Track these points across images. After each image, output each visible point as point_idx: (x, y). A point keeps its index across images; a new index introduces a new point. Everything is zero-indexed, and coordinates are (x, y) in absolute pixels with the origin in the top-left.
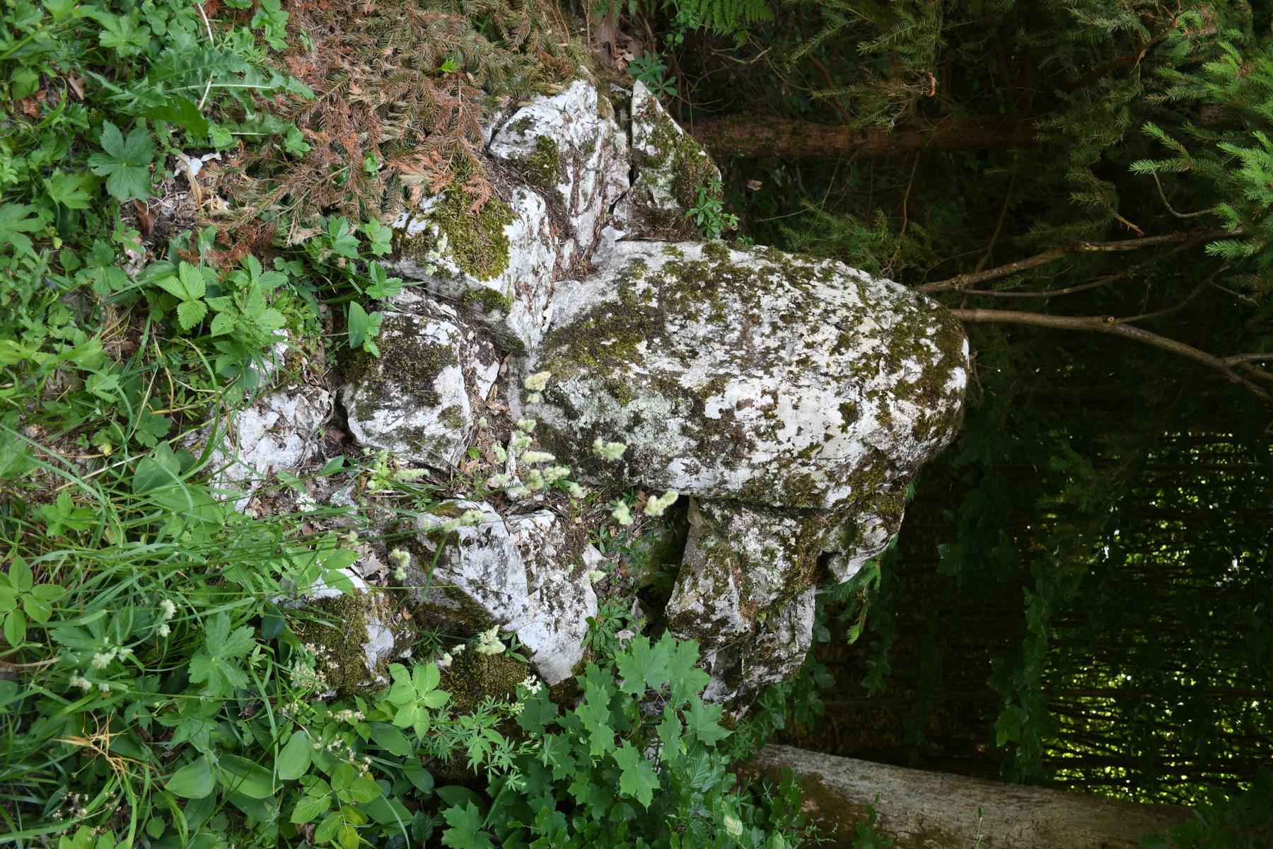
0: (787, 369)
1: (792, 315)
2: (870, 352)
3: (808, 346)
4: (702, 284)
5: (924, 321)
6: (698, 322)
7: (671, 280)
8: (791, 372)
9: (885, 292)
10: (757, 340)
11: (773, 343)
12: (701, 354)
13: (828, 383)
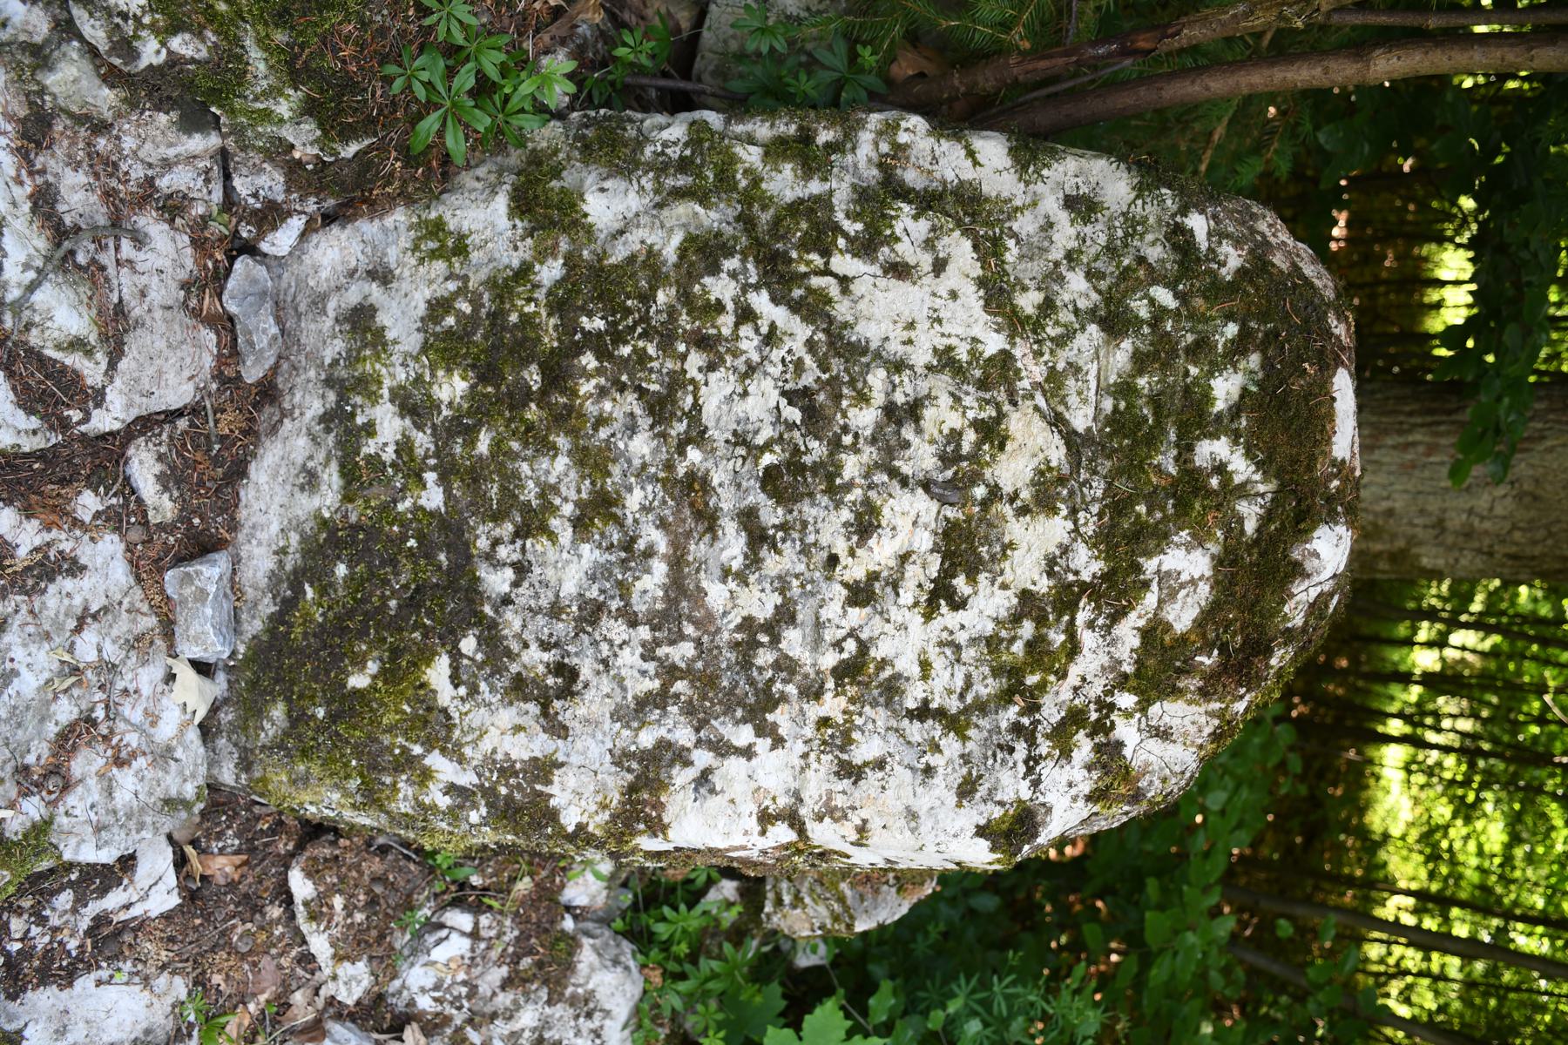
0: (814, 711)
1: (795, 465)
2: (1043, 585)
3: (860, 594)
4: (533, 377)
5: (1201, 348)
6: (552, 537)
7: (452, 388)
8: (824, 722)
9: (1066, 234)
10: (717, 594)
11: (760, 603)
12: (586, 672)
13: (936, 748)
